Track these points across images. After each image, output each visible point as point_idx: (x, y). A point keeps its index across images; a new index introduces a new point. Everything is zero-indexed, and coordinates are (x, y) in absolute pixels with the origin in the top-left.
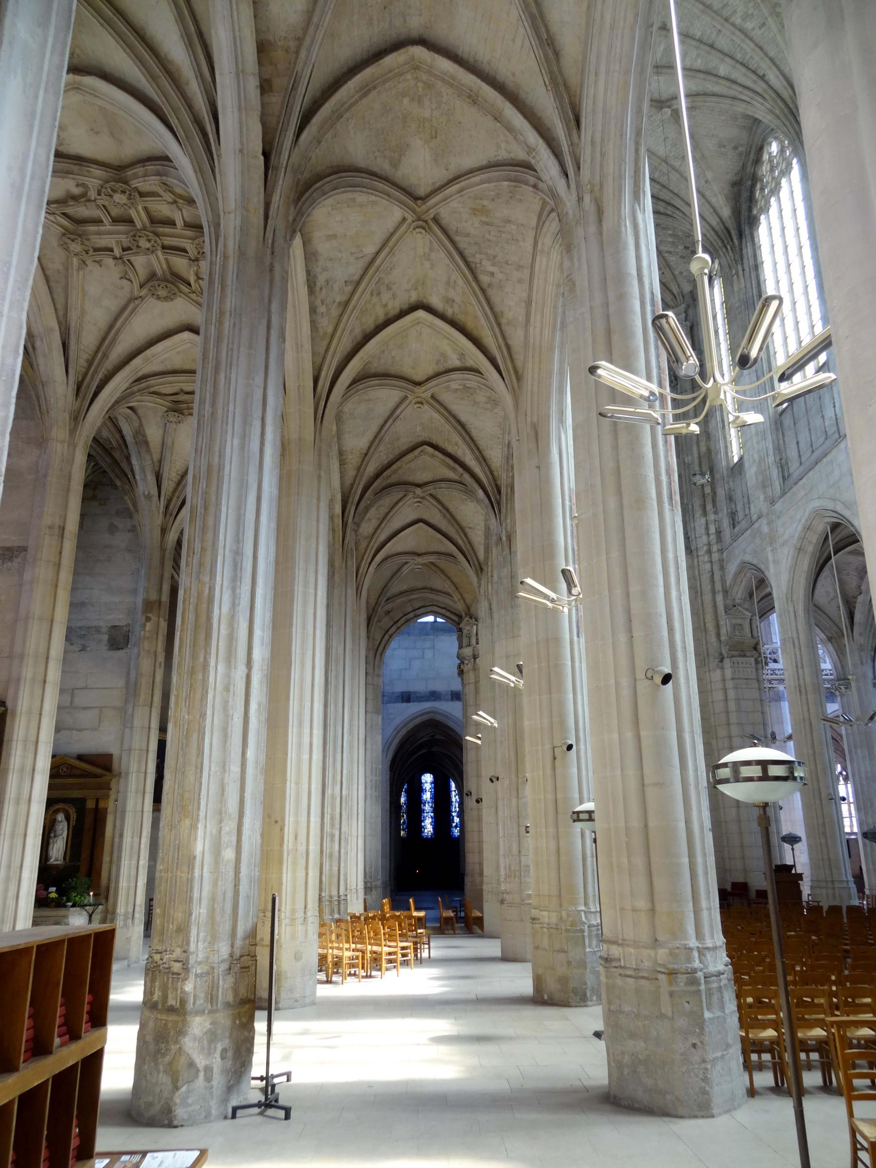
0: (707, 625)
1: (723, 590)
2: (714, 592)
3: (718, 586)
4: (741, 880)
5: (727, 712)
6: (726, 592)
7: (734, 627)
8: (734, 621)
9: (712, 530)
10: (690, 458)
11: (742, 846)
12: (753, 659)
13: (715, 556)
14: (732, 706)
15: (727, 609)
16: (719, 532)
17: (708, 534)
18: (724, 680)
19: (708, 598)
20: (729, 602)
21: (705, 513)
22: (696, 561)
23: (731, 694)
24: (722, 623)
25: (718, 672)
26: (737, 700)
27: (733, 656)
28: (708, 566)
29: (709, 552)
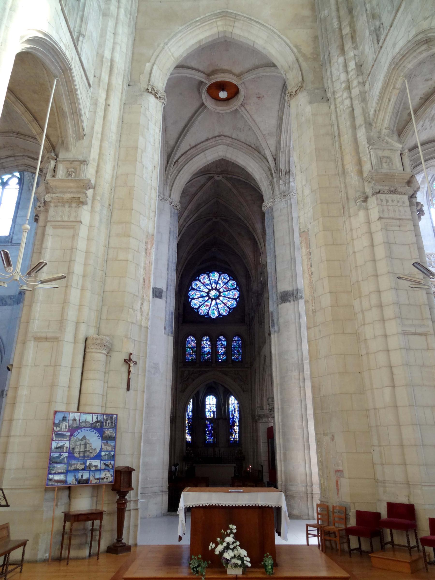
0: (346, 167)
1: (365, 122)
2: (354, 128)
3: (359, 120)
4: (402, 499)
5: (374, 261)
6: (369, 124)
7: (380, 159)
8: (380, 153)
9: (352, 65)
10: (326, 12)
11: (402, 446)
12: (406, 198)
13: (355, 92)
14: (380, 252)
15: (370, 141)
16: (359, 66)
17: (347, 72)
18: (369, 223)
19: (347, 138)
20: (374, 134)
21: (343, 51)
22: (332, 107)
23: (379, 238)
24: (365, 159)
25: (362, 214)
26: (388, 244)
27: (379, 193)
28: (347, 102)
29: (349, 88)
